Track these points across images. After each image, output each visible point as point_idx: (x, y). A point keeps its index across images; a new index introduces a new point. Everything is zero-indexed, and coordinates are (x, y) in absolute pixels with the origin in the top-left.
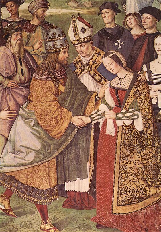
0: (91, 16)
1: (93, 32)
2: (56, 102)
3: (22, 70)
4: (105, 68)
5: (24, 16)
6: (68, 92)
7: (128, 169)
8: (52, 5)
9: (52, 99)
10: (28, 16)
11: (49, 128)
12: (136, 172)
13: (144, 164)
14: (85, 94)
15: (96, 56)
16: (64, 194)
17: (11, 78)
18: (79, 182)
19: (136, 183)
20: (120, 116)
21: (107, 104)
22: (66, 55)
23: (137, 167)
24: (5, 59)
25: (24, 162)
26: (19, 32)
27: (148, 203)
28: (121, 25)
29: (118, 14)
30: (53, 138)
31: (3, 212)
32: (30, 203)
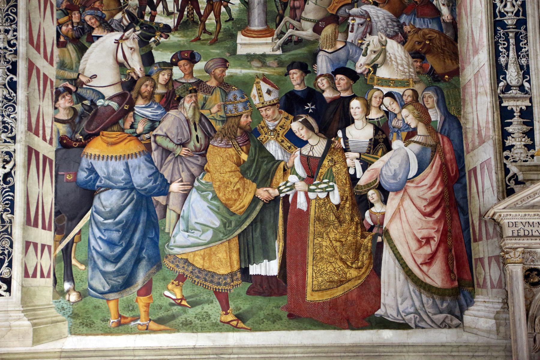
0: (278, 77)
1: (280, 93)
2: (238, 172)
3: (197, 136)
4: (294, 134)
5: (200, 76)
6: (251, 161)
7: (324, 247)
8: (232, 65)
9: (233, 168)
10: (205, 77)
11: (229, 202)
12: (333, 251)
13: (342, 242)
14: (271, 163)
15: (283, 121)
16: (248, 278)
17: (183, 145)
18: (266, 264)
19: (333, 264)
20: (312, 187)
21: (297, 174)
22: (249, 119)
23: (334, 245)
24: (177, 124)
25: (200, 241)
26: (193, 94)
27: (348, 287)
28: (312, 86)
29: (308, 75)
30: (235, 214)
31: (173, 302)
32: (207, 290)
